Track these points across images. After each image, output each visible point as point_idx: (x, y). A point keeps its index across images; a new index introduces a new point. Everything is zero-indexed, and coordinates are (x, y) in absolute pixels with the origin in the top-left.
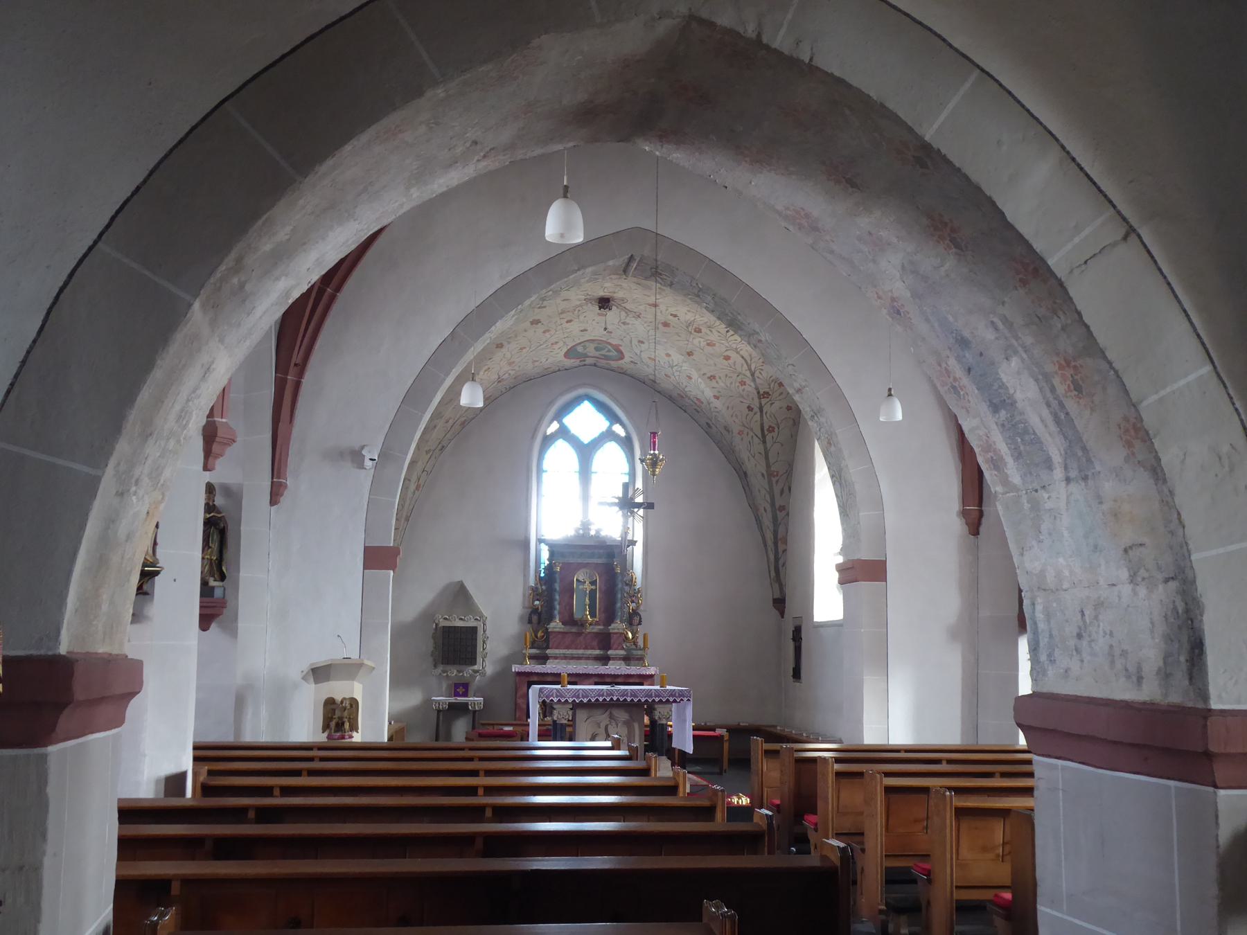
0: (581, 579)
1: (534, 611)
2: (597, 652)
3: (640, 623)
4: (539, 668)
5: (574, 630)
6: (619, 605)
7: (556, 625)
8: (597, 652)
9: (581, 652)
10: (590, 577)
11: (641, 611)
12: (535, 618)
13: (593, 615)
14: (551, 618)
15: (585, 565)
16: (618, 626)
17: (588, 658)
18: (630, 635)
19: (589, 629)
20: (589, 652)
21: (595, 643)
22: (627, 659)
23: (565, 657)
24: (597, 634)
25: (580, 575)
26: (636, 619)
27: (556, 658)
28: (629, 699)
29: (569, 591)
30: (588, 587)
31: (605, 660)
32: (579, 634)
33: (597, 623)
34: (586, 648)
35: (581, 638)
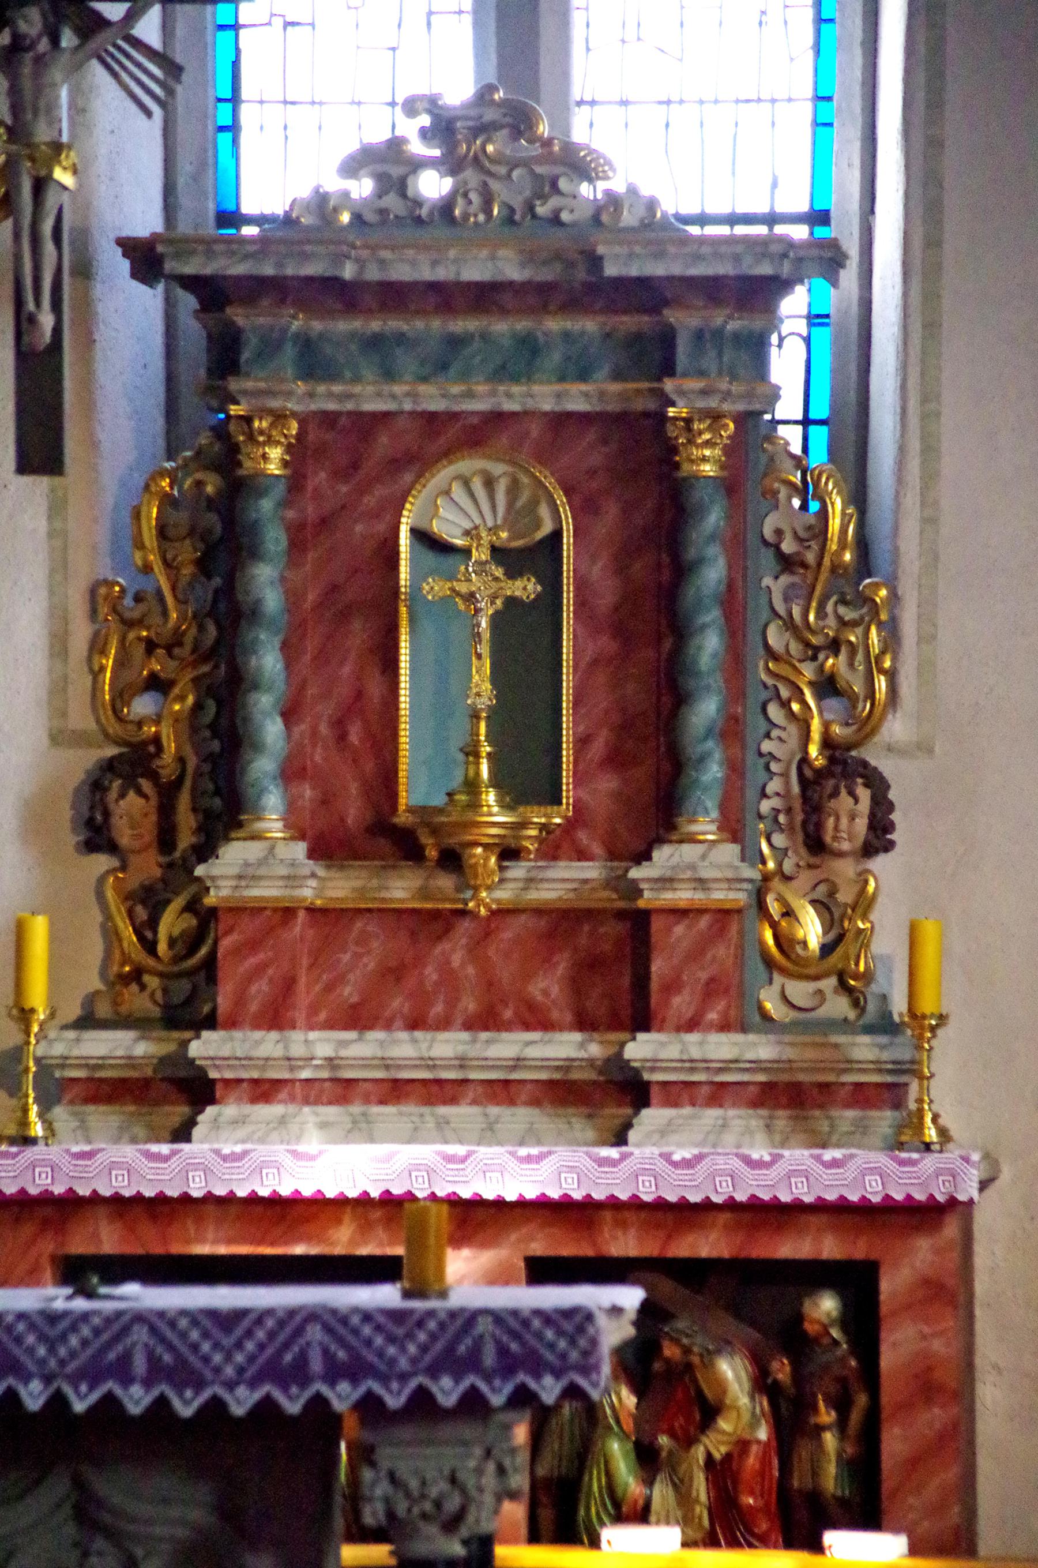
0: (449, 526)
1: (133, 762)
2: (566, 1047)
3: (879, 838)
4: (122, 1162)
5: (401, 888)
6: (706, 709)
7: (265, 862)
8: (566, 1047)
9: (446, 1047)
10: (520, 516)
11: (893, 746)
12: (131, 812)
13: (529, 777)
14: (227, 814)
15: (480, 433)
16: (697, 865)
17: (502, 1091)
18: (811, 930)
19: (499, 888)
20: (506, 1047)
21: (549, 986)
22: (793, 1098)
23: (340, 1089)
24: (562, 922)
25: (453, 503)
26: (849, 815)
27: (264, 1090)
28: (136, 1400)
29: (363, 609)
30: (488, 588)
31: (616, 1097)
32: (433, 923)
33: (556, 845)
34: (487, 1020)
35: (455, 950)
